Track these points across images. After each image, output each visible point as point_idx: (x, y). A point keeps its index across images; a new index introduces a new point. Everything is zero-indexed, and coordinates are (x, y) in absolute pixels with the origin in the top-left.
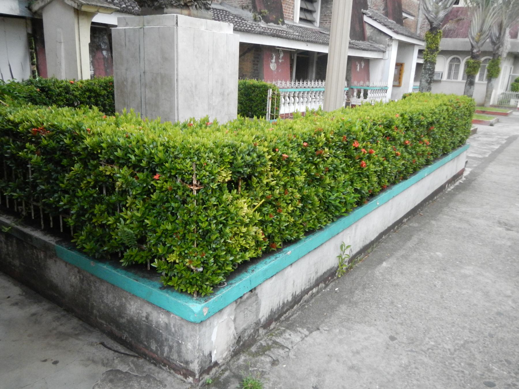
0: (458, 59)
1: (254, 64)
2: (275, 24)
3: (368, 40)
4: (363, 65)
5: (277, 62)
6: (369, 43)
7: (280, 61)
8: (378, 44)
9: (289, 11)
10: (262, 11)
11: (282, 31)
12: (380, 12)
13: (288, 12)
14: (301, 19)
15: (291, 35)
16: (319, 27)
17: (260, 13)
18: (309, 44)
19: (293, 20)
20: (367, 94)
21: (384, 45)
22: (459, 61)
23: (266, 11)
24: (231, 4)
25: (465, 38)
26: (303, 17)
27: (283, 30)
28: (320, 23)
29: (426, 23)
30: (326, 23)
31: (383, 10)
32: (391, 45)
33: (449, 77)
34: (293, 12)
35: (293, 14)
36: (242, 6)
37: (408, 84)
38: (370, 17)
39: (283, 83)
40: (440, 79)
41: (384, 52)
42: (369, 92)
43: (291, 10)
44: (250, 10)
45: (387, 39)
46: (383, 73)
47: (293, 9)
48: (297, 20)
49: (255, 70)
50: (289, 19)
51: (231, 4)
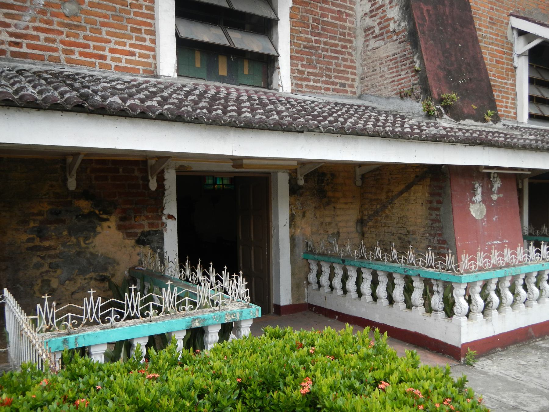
1: (430, 208)
2: (476, 120)
5: (486, 199)
7: (495, 197)
9: (507, 102)
10: (444, 96)
11: (493, 133)
13: (504, 104)
15: (518, 139)
17: (441, 101)
19: (516, 118)
23: (454, 95)
24: (378, 93)
27: (496, 132)
34: (514, 104)
35: (515, 108)
39: (507, 253)
43: (510, 101)
44: (417, 98)
47: (513, 99)
49: (434, 221)
50: (508, 117)
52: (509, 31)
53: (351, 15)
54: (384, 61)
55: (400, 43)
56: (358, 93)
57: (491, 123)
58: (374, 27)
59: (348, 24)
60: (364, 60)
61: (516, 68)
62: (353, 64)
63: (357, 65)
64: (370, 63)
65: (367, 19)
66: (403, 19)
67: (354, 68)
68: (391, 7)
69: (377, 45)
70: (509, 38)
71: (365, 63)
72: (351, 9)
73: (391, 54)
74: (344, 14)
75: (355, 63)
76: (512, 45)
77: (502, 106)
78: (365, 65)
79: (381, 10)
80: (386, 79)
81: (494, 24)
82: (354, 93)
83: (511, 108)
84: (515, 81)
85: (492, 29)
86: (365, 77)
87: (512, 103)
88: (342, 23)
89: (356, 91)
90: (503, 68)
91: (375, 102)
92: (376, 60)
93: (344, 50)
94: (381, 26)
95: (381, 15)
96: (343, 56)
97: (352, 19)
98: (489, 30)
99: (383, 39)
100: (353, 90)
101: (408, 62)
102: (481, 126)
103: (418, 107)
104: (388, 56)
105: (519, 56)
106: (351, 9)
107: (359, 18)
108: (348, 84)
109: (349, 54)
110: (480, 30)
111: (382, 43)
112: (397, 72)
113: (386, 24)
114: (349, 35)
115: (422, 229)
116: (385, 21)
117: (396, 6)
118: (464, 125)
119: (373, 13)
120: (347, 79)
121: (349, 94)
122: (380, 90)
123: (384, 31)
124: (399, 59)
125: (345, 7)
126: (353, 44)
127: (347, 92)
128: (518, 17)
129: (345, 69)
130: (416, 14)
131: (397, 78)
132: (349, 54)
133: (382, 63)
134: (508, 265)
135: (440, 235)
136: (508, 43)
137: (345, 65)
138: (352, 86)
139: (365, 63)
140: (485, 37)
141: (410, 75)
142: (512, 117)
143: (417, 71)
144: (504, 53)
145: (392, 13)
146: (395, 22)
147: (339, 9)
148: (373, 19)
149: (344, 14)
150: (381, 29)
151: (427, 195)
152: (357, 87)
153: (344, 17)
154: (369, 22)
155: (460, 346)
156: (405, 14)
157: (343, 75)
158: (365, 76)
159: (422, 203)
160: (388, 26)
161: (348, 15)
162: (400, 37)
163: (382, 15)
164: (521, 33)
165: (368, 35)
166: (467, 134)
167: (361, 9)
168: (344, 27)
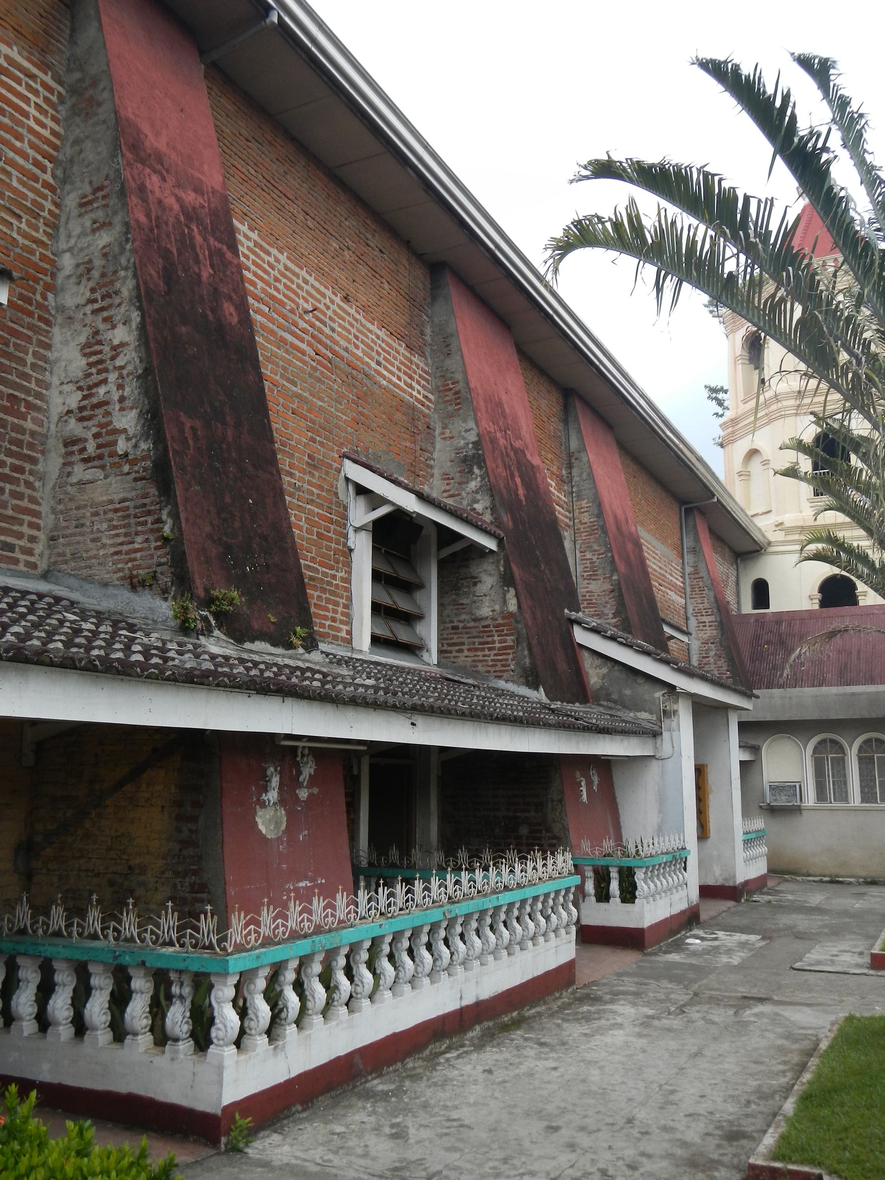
0: (834, 742)
2: (274, 645)
3: (597, 701)
4: (596, 779)
5: (287, 800)
6: (601, 709)
7: (303, 794)
8: (630, 710)
10: (215, 593)
11: (303, 671)
12: (610, 622)
13: (330, 614)
14: (376, 640)
16: (439, 665)
17: (208, 602)
18: (419, 720)
19: (349, 641)
20: (635, 887)
21: (651, 713)
22: (842, 750)
23: (235, 594)
24: (85, 572)
25: (821, 685)
26: (381, 632)
27: (309, 669)
28: (440, 652)
29: (712, 653)
30: (461, 651)
31: (615, 615)
32: (675, 712)
33: (821, 795)
35: (349, 623)
36: (131, 577)
37: (731, 828)
38: (595, 630)
39: (318, 904)
40: (798, 803)
41: (656, 734)
42: (639, 876)
43: (340, 609)
44: (164, 592)
45: (659, 694)
46: (661, 801)
47: (346, 606)
48: (363, 641)
50: (336, 638)
51: (85, 572)
52: (341, 484)
53: (38, 409)
54: (101, 510)
55: (136, 480)
56: (43, 566)
57: (301, 650)
58: (86, 440)
59: (29, 425)
60: (60, 501)
61: (351, 550)
62: (34, 507)
63: (44, 509)
64: (71, 509)
65: (72, 421)
66: (146, 436)
67: (37, 514)
68: (122, 409)
69: (89, 475)
70: (342, 496)
71: (61, 507)
72: (38, 396)
73: (116, 498)
74: (23, 404)
75: (39, 504)
76: (346, 508)
77: (325, 618)
78: (62, 512)
79: (100, 411)
80: (104, 546)
81: (315, 467)
82: (34, 566)
83: (342, 622)
84: (349, 573)
85: (313, 476)
86: (59, 536)
87: (343, 614)
88: (16, 421)
89: (38, 563)
90: (329, 548)
91: (77, 590)
92: (85, 506)
93: (16, 475)
94: (100, 441)
95: (101, 419)
96: (14, 487)
97: (40, 416)
98: (307, 477)
99: (103, 467)
100: (32, 559)
101: (150, 519)
102: (284, 656)
103: (165, 609)
104: (111, 502)
105: (357, 530)
106: (38, 396)
107: (54, 418)
108: (21, 547)
109: (29, 485)
110: (291, 475)
111: (100, 474)
112: (126, 535)
113: (111, 438)
114: (31, 446)
115: (161, 862)
116: (109, 433)
117: (132, 408)
118: (251, 651)
119: (85, 413)
120: (20, 535)
121: (21, 567)
122: (90, 567)
123: (105, 451)
124: (132, 511)
125: (28, 391)
126: (38, 467)
127: (16, 561)
128: (355, 461)
129: (16, 515)
130: (170, 431)
131: (125, 548)
132: (29, 485)
133: (96, 514)
134: (318, 930)
135: (195, 873)
136: (339, 504)
137: (17, 506)
138: (29, 552)
139: (61, 507)
140: (299, 489)
141: (153, 545)
142: (344, 640)
143: (166, 540)
144: (331, 521)
145: (124, 420)
146: (128, 439)
147: (11, 391)
148: (85, 424)
149: (23, 404)
150: (99, 446)
151: (173, 789)
152: (41, 555)
153: (23, 410)
154: (74, 427)
155: (219, 1112)
156: (149, 428)
157: (11, 527)
158: (60, 533)
159: (163, 807)
160: (115, 443)
161: (30, 406)
162: (136, 468)
163: (104, 420)
164: (361, 490)
165: (72, 453)
166: (253, 672)
167: (60, 400)
168: (21, 430)
